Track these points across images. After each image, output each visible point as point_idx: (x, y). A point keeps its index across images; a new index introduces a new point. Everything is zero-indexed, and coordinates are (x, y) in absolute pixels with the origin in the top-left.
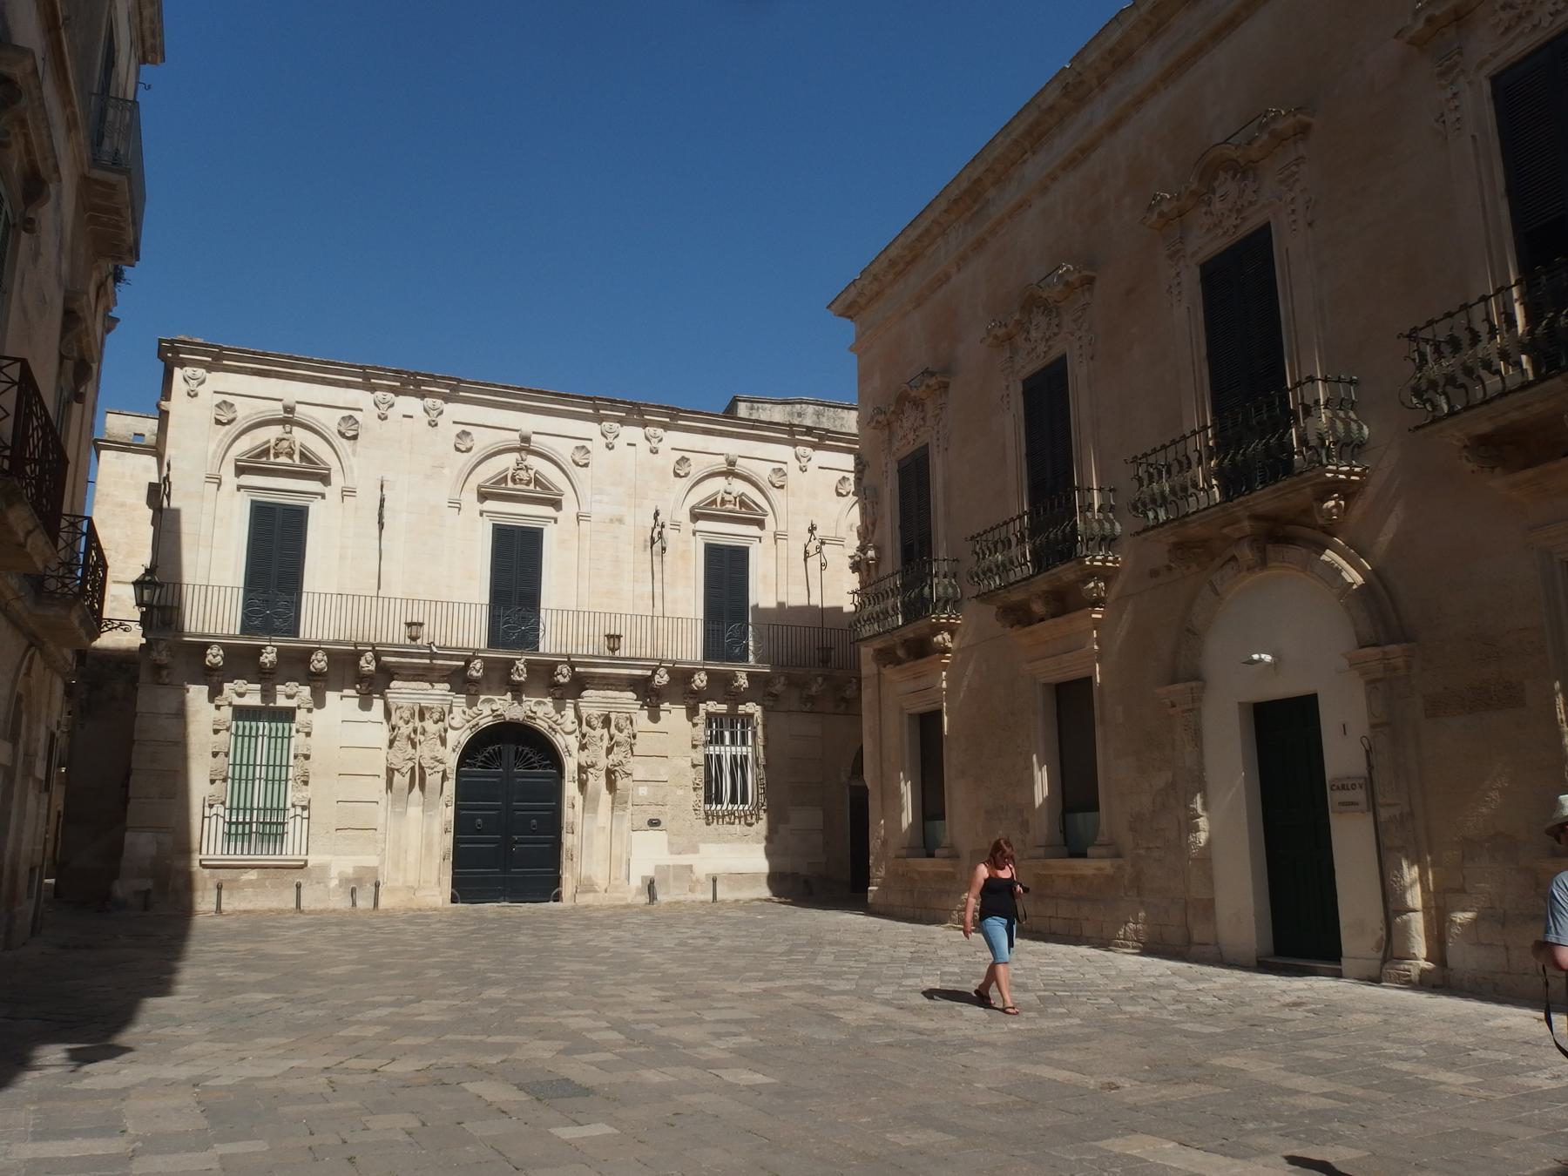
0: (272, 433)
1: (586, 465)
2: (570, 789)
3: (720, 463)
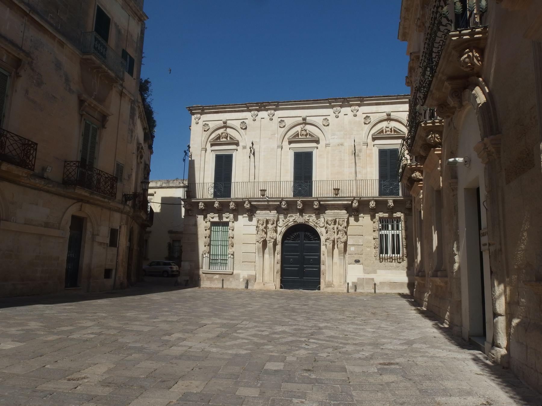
0: (220, 132)
1: (328, 125)
2: (323, 248)
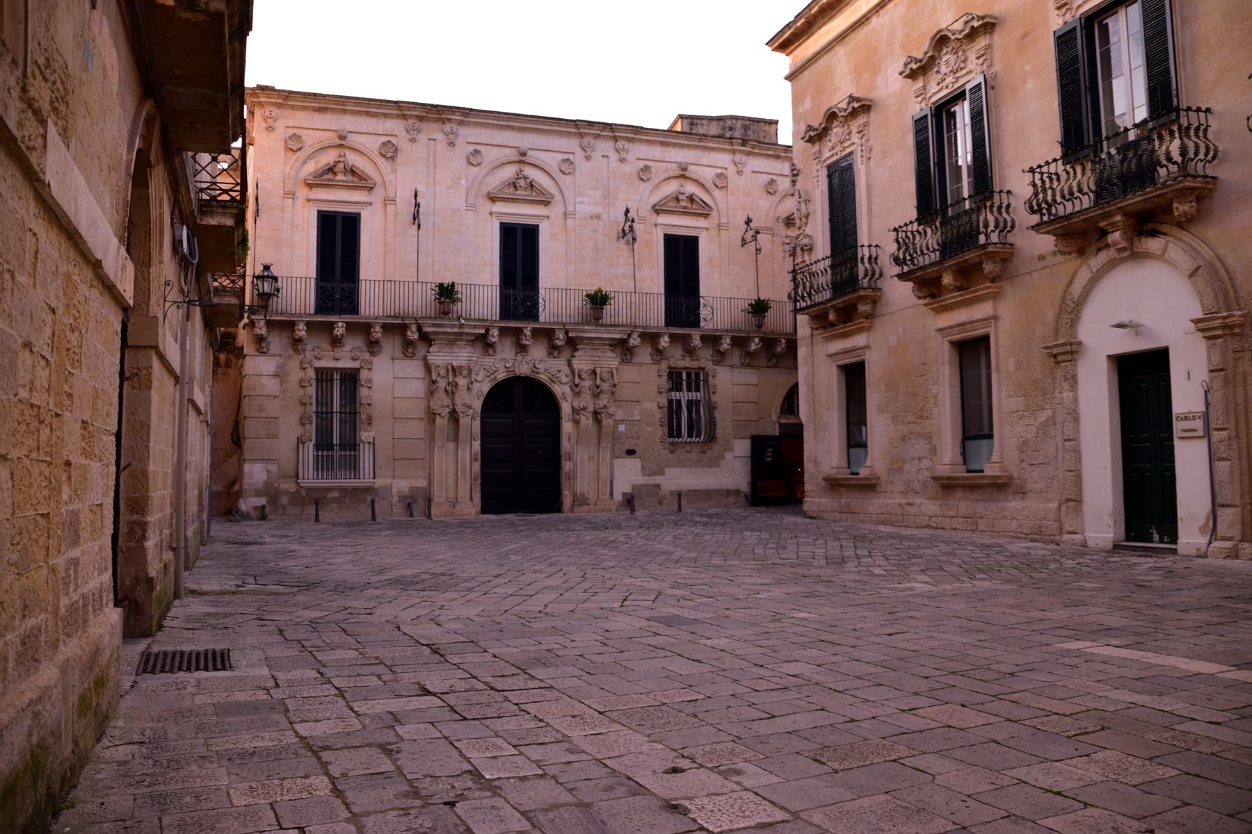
0: (329, 157)
2: (567, 427)
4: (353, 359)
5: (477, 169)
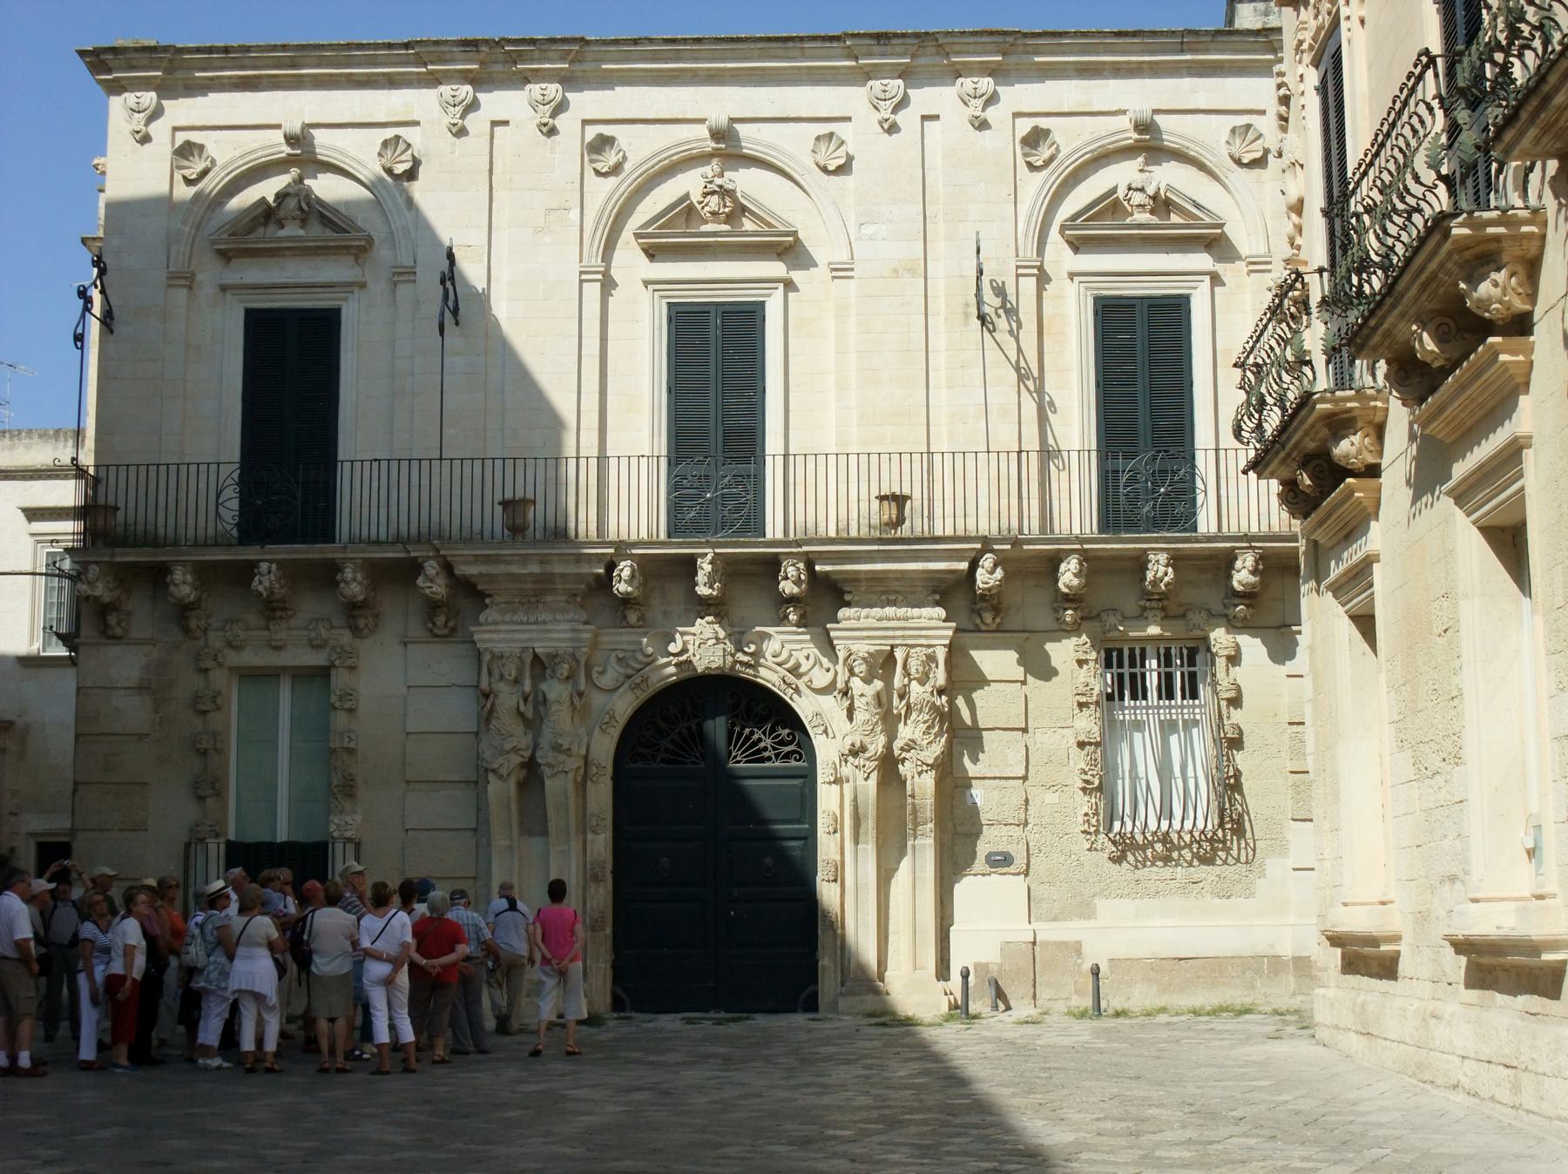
1: (844, 169)
2: (828, 799)
3: (1122, 130)
4: (316, 646)
5: (612, 181)
